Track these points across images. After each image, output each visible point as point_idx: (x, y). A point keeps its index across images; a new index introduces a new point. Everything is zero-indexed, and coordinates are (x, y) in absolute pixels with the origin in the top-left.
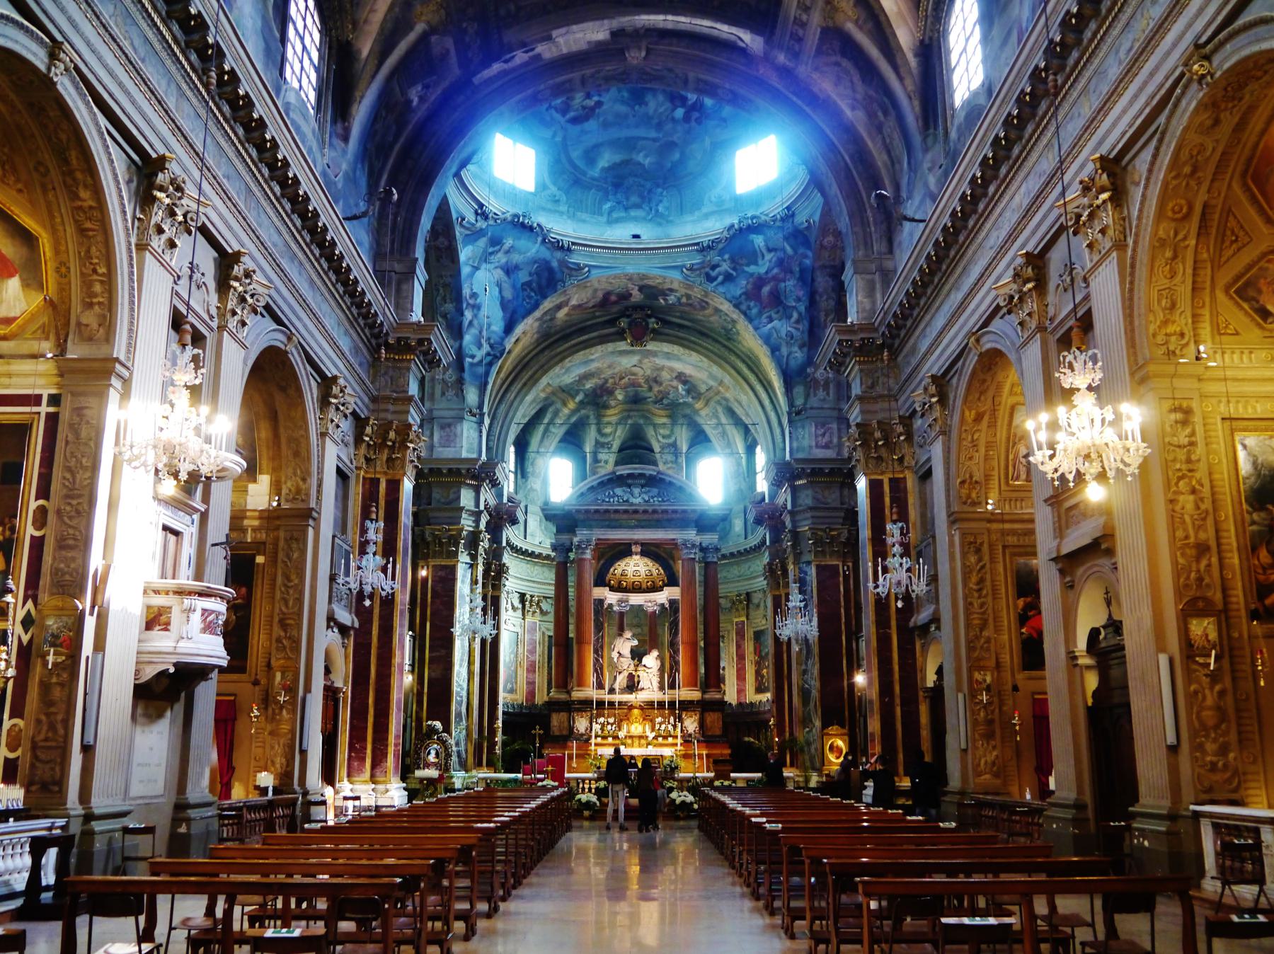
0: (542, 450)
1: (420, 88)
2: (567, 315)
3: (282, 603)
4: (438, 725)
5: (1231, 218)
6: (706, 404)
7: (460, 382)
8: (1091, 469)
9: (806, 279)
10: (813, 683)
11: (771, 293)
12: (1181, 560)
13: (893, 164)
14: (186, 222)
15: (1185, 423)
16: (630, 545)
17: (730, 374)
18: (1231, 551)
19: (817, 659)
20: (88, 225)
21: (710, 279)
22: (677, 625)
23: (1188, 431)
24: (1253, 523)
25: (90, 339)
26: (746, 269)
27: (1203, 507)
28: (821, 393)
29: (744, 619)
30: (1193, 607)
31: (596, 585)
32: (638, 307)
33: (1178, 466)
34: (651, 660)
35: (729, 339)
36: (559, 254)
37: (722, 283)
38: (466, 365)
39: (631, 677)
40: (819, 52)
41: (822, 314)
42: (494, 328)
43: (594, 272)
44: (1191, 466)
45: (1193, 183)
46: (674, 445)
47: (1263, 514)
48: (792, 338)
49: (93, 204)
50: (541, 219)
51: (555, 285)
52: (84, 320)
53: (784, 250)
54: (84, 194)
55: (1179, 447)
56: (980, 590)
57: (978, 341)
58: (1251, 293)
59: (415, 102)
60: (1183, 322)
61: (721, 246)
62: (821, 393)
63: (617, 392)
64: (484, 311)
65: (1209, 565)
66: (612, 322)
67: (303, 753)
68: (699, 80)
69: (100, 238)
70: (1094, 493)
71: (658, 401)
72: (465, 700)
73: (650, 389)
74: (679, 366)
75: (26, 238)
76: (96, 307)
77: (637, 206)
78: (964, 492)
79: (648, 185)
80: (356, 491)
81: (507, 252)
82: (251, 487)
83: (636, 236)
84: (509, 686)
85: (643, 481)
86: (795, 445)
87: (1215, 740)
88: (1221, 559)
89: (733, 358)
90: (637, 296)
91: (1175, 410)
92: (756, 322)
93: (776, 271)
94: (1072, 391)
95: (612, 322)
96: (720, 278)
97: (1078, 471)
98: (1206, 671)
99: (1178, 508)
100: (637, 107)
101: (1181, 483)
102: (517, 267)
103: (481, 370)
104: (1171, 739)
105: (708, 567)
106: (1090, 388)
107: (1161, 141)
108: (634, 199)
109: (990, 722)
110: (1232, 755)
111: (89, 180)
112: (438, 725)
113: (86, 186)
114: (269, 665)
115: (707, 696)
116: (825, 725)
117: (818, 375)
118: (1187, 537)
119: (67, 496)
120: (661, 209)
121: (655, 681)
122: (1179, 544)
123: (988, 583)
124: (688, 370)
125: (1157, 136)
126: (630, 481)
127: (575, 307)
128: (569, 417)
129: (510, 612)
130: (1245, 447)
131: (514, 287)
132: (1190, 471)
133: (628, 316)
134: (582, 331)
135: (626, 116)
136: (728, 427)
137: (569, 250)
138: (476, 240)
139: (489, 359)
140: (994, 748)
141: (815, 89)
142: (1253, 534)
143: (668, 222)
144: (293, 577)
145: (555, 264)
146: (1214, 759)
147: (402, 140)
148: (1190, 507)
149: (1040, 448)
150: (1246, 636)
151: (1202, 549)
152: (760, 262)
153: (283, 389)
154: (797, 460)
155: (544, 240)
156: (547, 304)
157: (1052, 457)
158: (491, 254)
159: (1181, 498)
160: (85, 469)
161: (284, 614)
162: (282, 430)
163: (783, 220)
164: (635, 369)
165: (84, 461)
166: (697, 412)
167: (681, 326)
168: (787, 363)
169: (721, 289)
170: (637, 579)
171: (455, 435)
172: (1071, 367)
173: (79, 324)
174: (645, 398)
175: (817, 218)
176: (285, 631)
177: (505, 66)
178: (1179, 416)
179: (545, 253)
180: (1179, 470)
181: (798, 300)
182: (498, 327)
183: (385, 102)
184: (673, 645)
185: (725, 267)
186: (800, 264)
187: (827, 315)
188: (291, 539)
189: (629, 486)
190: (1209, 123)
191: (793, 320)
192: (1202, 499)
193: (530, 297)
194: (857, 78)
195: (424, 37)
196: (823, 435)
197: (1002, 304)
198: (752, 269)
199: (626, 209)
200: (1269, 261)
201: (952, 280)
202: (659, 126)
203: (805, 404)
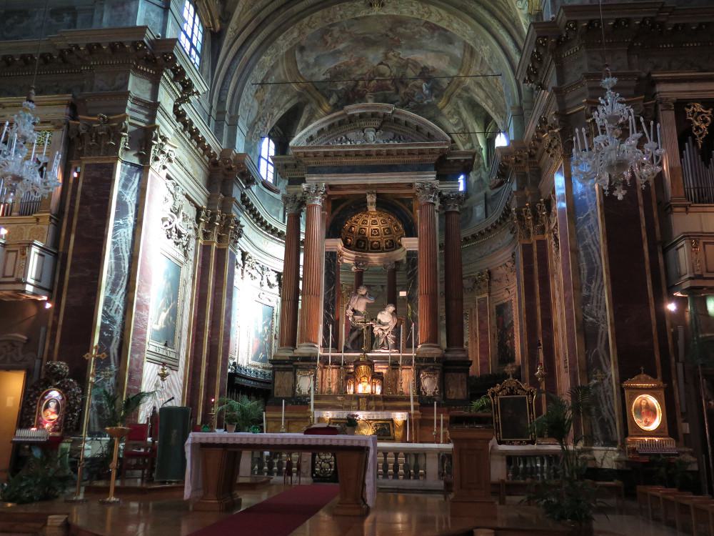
4: (62, 366)
10: (601, 313)
29: (486, 295)
72: (117, 337)
73: (397, 91)
105: (446, 215)
112: (62, 366)
116: (627, 372)
129: (266, 287)
164: (383, 68)
166: (439, 112)
171: (129, 14)
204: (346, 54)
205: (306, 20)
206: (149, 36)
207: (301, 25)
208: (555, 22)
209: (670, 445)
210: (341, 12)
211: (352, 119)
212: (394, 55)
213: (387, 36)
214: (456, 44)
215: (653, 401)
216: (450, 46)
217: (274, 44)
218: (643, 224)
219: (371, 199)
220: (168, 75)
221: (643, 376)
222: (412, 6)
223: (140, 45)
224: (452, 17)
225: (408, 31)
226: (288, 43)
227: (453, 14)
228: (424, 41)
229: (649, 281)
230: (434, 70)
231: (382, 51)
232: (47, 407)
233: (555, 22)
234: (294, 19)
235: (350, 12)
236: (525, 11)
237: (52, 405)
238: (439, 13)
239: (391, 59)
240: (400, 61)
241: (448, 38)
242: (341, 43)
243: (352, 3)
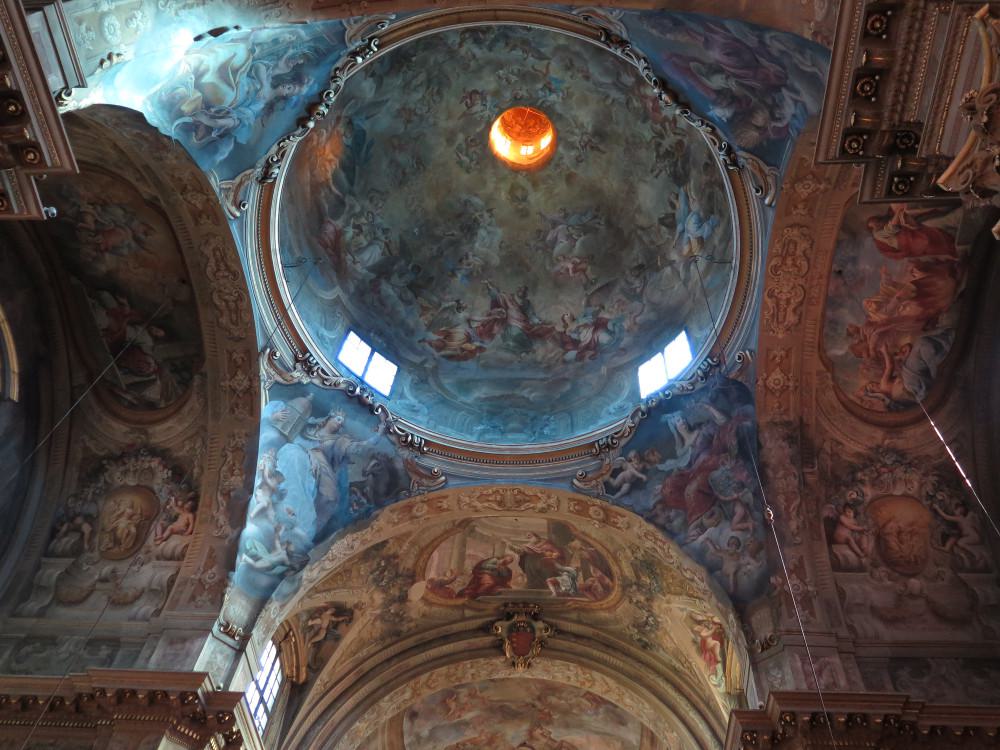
7: (222, 584)
9: (748, 448)
11: (699, 491)
17: (649, 701)
21: (611, 490)
26: (661, 467)
36: (406, 453)
37: (628, 493)
42: (298, 531)
43: (452, 482)
48: (738, 544)
51: (398, 493)
53: (710, 421)
61: (623, 442)
64: (286, 504)
66: (486, 629)
77: (520, 431)
79: (532, 414)
81: (335, 432)
89: (651, 677)
92: (682, 536)
93: (703, 457)
95: (486, 629)
96: (625, 487)
102: (346, 458)
103: (264, 581)
108: (513, 425)
127: (438, 587)
131: (339, 484)
134: (446, 639)
135: (511, 362)
137: (420, 449)
138: (292, 398)
139: (279, 569)
145: (399, 465)
152: (679, 452)
154: (782, 697)
155: (387, 431)
158: (313, 426)
163: (706, 375)
167: (578, 637)
168: (736, 584)
169: (627, 501)
179: (387, 447)
181: (742, 485)
182: (304, 531)
185: (631, 470)
191: (736, 518)
193: (360, 504)
196: (820, 673)
198: (669, 464)
199: (503, 433)
202: (549, 368)
203: (775, 631)
204: (475, 728)
205: (424, 678)
206: (207, 686)
207: (416, 683)
208: (765, 712)
210: (473, 671)
212: (542, 734)
213: (534, 706)
214: (629, 725)
216: (622, 728)
217: (376, 706)
220: (217, 741)
222: (569, 670)
223: (191, 698)
224: (623, 689)
225: (563, 702)
226: (395, 706)
227: (624, 684)
228: (585, 718)
231: (525, 726)
233: (765, 712)
234: (409, 674)
235: (484, 672)
236: (722, 689)
238: (605, 681)
239: (538, 740)
240: (550, 742)
241: (620, 719)
242: (469, 711)
243: (487, 661)
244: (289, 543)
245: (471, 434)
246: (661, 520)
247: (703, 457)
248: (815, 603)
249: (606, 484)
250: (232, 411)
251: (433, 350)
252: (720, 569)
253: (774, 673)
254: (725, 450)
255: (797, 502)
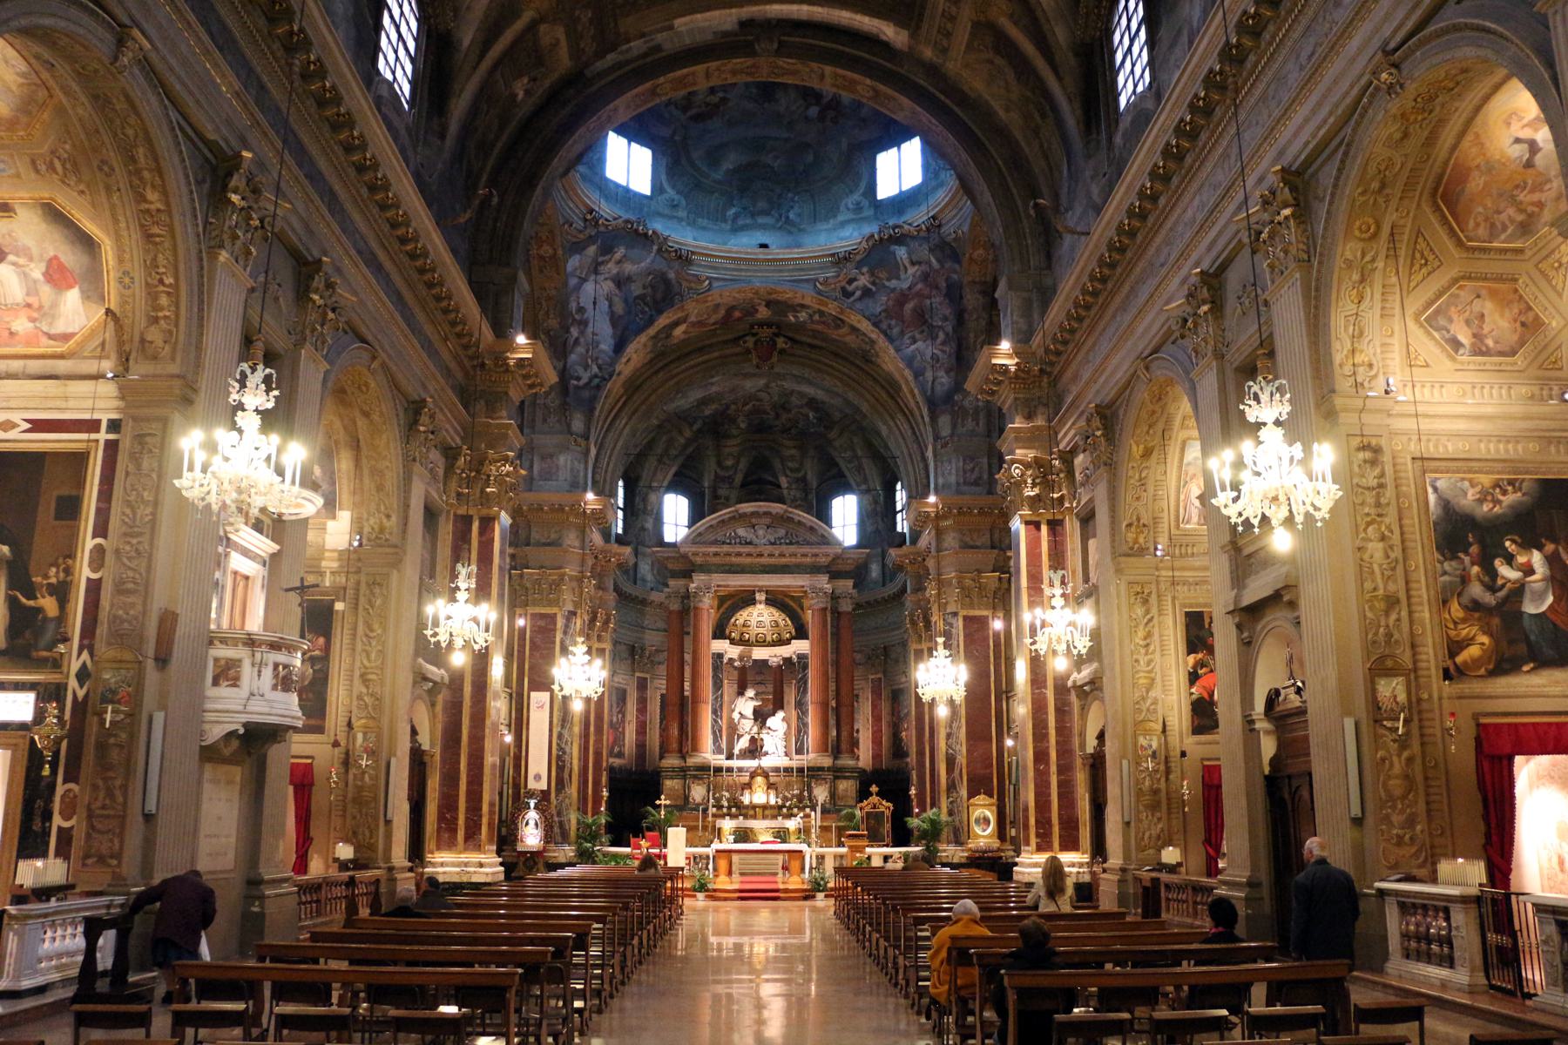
0: (655, 484)
1: (526, 80)
2: (684, 332)
3: (364, 655)
5: (1420, 240)
6: (841, 434)
8: (1277, 515)
9: (954, 294)
10: (958, 747)
11: (914, 310)
12: (1369, 614)
13: (1051, 169)
14: (262, 227)
15: (1373, 463)
16: (754, 593)
18: (1421, 604)
19: (963, 721)
20: (156, 230)
22: (806, 683)
23: (1377, 471)
24: (1445, 573)
25: (155, 358)
26: (887, 284)
27: (1393, 555)
28: (970, 424)
30: (1380, 668)
31: (715, 637)
32: (761, 324)
33: (1367, 510)
34: (776, 722)
35: (868, 361)
37: (860, 299)
38: (571, 390)
39: (753, 740)
40: (969, 47)
41: (972, 335)
42: (603, 347)
44: (1380, 511)
45: (1381, 200)
46: (804, 480)
47: (1454, 563)
48: (938, 361)
49: (162, 208)
50: (658, 226)
52: (149, 338)
53: (929, 263)
54: (152, 196)
55: (1368, 489)
56: (1147, 645)
57: (1147, 368)
58: (1442, 322)
59: (521, 95)
60: (1372, 351)
61: (858, 258)
62: (970, 424)
63: (741, 418)
65: (1398, 620)
67: (388, 822)
68: (836, 75)
69: (167, 245)
70: (1281, 542)
71: (785, 431)
73: (777, 416)
74: (810, 391)
75: (87, 243)
76: (162, 322)
77: (766, 213)
78: (1131, 536)
80: (446, 530)
81: (619, 262)
82: (330, 524)
83: (764, 246)
84: (616, 749)
85: (768, 521)
86: (941, 481)
87: (1402, 812)
88: (1410, 613)
90: (763, 313)
91: (1363, 448)
92: (897, 343)
94: (1259, 425)
96: (858, 293)
97: (1263, 515)
98: (1394, 736)
99: (1366, 557)
100: (766, 105)
101: (1370, 528)
102: (629, 279)
104: (1356, 811)
106: (1278, 423)
107: (1346, 154)
108: (762, 205)
109: (1156, 792)
110: (1419, 828)
111: (158, 181)
113: (153, 186)
114: (349, 725)
115: (840, 762)
117: (966, 403)
118: (1375, 589)
119: (125, 534)
120: (791, 215)
121: (781, 744)
122: (1367, 596)
123: (1156, 637)
124: (820, 395)
125: (1343, 147)
126: (754, 520)
127: (693, 324)
128: (685, 447)
130: (1435, 489)
131: (626, 301)
132: (1380, 515)
133: (754, 335)
136: (864, 460)
139: (596, 381)
140: (1159, 819)
141: (965, 88)
142: (1444, 588)
143: (800, 230)
144: (376, 626)
145: (672, 275)
146: (1400, 832)
147: (504, 138)
148: (1379, 555)
149: (1223, 489)
150: (1436, 696)
151: (1392, 602)
152: (903, 276)
153: (366, 414)
155: (660, 250)
156: (663, 321)
157: (1235, 500)
158: (603, 263)
159: (1370, 545)
160: (146, 503)
161: (365, 667)
162: (364, 461)
164: (763, 395)
165: (146, 494)
168: (933, 388)
169: (858, 305)
170: (761, 630)
172: (1257, 398)
173: (143, 341)
174: (771, 427)
175: (966, 228)
176: (367, 687)
177: (621, 58)
178: (1368, 455)
179: (661, 265)
180: (1368, 515)
181: (945, 319)
182: (606, 346)
183: (485, 93)
184: (800, 705)
185: (863, 281)
186: (947, 280)
187: (976, 337)
188: (372, 584)
189: (753, 527)
190: (1398, 136)
191: (939, 341)
192: (1391, 547)
193: (643, 312)
194: (1011, 75)
195: (532, 27)
196: (972, 470)
197: (1174, 328)
198: (893, 283)
199: (753, 215)
200: (1460, 288)
201: (1118, 300)
209: (996, 844)
211: (743, 516)
215: (988, 814)
218: (992, 679)
219: (760, 597)
221: (982, 796)
229: (994, 724)
230: (823, 402)
232: (527, 824)
237: (532, 823)
244: (597, 359)
245: (725, 221)
246: (884, 326)
247: (920, 286)
248: (982, 416)
249: (843, 289)
250: (541, 271)
251: (676, 113)
252: (923, 374)
253: (946, 464)
254: (937, 288)
255: (983, 337)
